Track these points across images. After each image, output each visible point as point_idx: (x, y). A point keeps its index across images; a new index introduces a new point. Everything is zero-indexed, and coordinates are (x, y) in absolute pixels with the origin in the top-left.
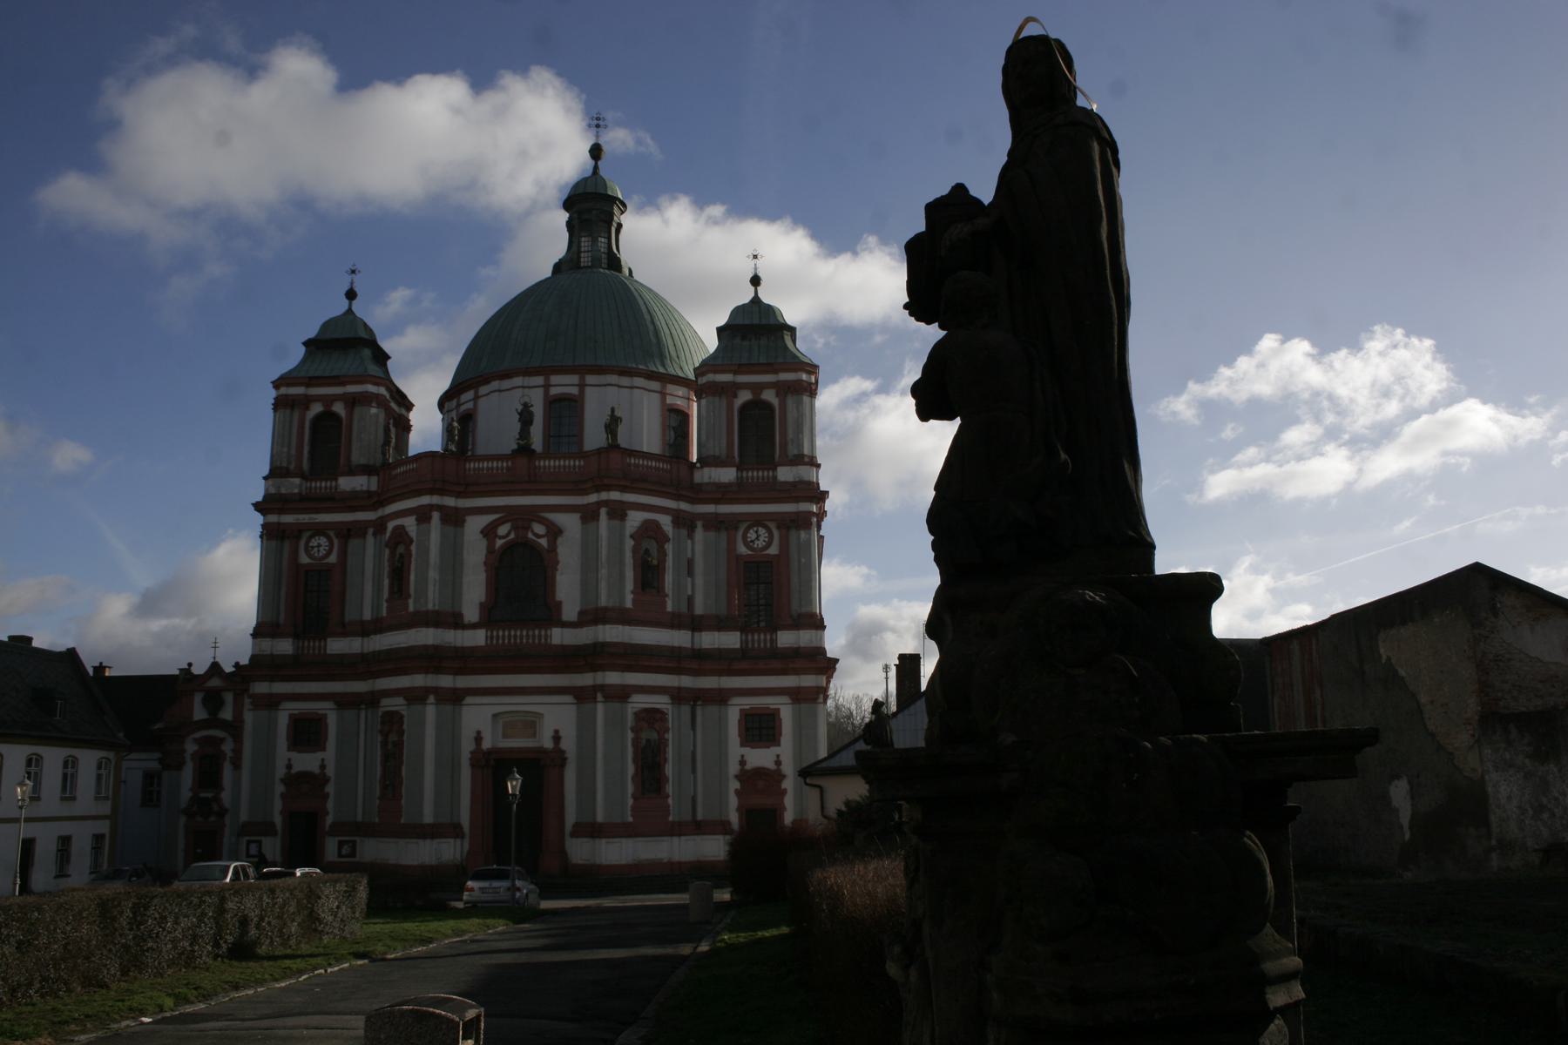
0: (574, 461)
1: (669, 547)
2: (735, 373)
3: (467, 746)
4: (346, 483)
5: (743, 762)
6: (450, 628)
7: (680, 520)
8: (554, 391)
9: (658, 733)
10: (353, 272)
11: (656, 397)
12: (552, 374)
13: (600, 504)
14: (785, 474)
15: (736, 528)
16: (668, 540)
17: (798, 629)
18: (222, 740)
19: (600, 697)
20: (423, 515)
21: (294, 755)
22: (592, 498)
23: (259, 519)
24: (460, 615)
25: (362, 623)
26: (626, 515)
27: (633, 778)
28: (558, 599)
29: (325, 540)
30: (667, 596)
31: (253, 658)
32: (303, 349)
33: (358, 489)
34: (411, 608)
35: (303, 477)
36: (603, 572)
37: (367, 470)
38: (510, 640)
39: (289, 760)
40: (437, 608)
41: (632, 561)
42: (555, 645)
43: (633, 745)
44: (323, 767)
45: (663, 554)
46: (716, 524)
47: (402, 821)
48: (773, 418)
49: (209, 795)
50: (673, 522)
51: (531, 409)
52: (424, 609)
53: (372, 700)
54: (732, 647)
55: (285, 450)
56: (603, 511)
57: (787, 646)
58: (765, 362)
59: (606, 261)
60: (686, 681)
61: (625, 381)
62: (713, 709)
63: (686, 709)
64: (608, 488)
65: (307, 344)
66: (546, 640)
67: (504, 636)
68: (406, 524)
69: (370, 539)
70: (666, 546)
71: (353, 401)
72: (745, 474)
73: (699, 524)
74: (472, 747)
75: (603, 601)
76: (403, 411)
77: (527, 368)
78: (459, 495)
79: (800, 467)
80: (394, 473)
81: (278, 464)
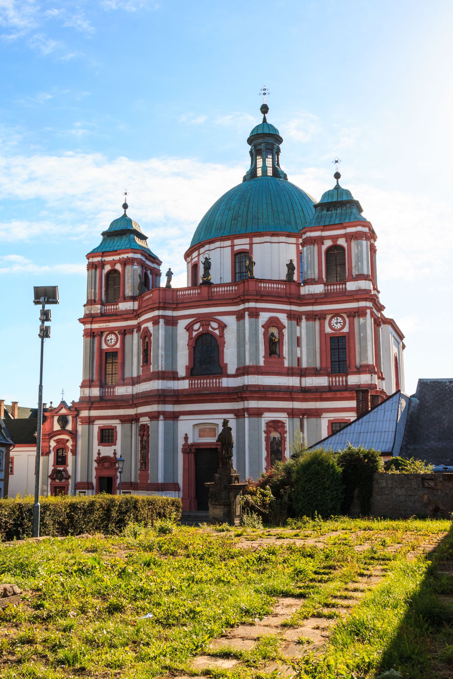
0: (232, 287)
1: (285, 332)
2: (322, 230)
3: (181, 442)
4: (123, 306)
6: (170, 380)
7: (291, 316)
8: (236, 248)
9: (280, 434)
10: (126, 194)
11: (295, 246)
12: (234, 239)
13: (245, 310)
14: (351, 286)
15: (325, 319)
16: (285, 327)
17: (360, 374)
18: (68, 441)
19: (246, 415)
20: (155, 321)
21: (101, 448)
22: (241, 307)
23: (82, 327)
24: (177, 373)
25: (132, 378)
26: (259, 315)
27: (266, 459)
28: (225, 362)
29: (114, 336)
30: (284, 358)
31: (82, 399)
32: (101, 237)
33: (128, 309)
34: (151, 371)
35: (102, 304)
36: (247, 347)
37: (133, 299)
38: (201, 385)
39: (99, 450)
40: (163, 369)
41: (263, 340)
42: (224, 387)
43: (266, 440)
44: (115, 454)
45: (281, 335)
46: (311, 316)
47: (149, 482)
48: (345, 255)
49: (61, 469)
50: (287, 317)
51: (209, 260)
52: (157, 370)
53: (135, 419)
54: (322, 385)
55: (93, 290)
56: (247, 313)
57: (354, 384)
58: (338, 223)
59: (271, 172)
60: (297, 405)
61: (275, 239)
62: (313, 420)
63: (297, 421)
64: (248, 301)
65: (103, 234)
66: (219, 384)
67: (198, 383)
68: (148, 326)
69: (136, 335)
70: (283, 331)
71: (125, 263)
72: (329, 288)
73: (304, 317)
74: (183, 442)
75: (247, 363)
76: (155, 266)
77: (222, 237)
78: (174, 309)
79: (359, 281)
80: (143, 299)
81: (90, 298)
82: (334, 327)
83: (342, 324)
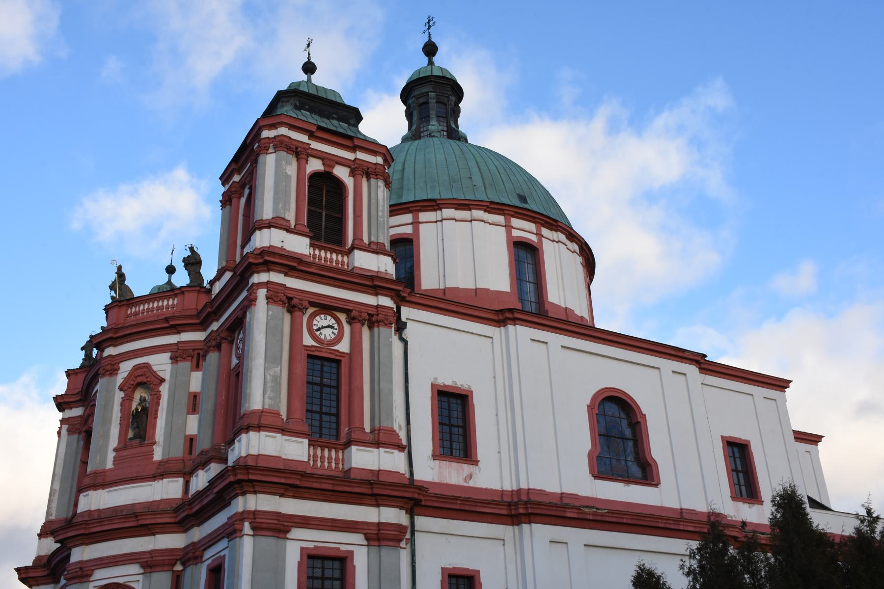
15: (303, 310)
82: (318, 333)
83: (336, 332)
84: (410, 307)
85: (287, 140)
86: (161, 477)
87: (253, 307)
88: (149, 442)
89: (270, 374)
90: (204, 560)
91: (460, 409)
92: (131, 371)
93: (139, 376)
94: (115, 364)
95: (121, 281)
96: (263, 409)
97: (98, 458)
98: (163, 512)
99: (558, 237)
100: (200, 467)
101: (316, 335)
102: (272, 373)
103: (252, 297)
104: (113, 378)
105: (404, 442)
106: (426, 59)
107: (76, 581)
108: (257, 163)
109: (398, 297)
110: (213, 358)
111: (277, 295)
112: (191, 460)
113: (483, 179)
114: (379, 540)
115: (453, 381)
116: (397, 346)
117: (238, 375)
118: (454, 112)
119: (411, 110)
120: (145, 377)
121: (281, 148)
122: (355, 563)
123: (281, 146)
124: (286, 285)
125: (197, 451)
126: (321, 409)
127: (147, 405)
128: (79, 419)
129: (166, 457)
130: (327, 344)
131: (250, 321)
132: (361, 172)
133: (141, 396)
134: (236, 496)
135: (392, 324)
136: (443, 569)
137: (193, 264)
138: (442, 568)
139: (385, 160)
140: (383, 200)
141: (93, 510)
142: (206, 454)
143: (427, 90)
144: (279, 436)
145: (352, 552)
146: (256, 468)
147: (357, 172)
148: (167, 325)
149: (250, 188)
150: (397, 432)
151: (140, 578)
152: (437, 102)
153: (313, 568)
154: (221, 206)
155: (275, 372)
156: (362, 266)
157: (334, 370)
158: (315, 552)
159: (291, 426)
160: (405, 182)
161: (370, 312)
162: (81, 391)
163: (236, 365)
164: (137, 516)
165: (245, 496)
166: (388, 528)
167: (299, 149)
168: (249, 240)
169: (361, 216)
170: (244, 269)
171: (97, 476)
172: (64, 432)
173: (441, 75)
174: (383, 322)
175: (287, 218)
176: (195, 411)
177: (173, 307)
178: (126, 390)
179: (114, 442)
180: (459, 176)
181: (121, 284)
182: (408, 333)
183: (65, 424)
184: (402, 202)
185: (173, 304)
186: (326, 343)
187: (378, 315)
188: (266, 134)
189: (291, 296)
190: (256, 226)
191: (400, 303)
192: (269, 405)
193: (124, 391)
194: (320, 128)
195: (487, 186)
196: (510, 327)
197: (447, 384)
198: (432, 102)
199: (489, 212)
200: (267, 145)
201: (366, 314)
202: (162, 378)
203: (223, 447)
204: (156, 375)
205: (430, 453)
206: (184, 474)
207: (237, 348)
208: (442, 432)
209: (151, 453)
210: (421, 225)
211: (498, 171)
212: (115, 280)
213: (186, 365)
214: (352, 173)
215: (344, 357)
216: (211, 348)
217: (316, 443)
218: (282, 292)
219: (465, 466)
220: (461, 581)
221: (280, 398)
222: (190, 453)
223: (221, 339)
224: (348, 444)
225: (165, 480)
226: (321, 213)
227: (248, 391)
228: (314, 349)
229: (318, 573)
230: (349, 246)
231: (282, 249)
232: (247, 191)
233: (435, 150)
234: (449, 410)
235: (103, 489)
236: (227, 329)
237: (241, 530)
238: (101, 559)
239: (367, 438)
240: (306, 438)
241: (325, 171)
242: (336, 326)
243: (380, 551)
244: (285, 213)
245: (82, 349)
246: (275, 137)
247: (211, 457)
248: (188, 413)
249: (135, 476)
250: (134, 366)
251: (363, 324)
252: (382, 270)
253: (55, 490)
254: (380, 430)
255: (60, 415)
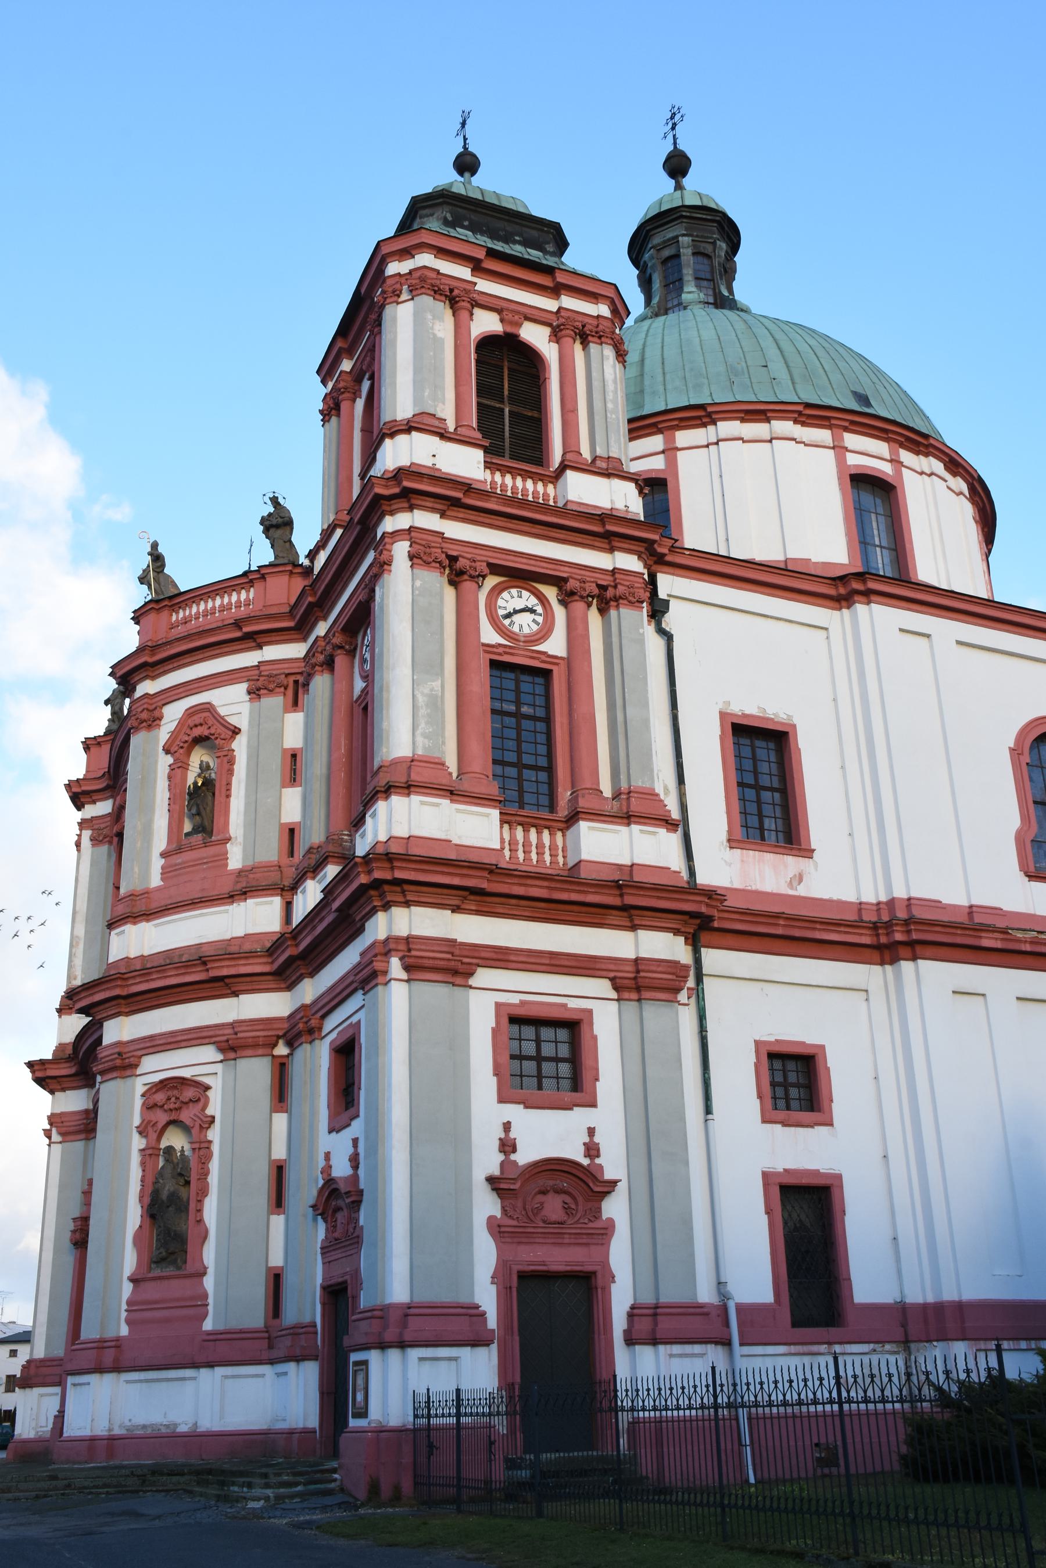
5: (507, 1146)
82: (507, 622)
83: (540, 619)
84: (673, 574)
85: (433, 275)
86: (243, 897)
87: (386, 576)
88: (219, 838)
89: (422, 694)
90: (323, 1034)
91: (773, 758)
92: (181, 718)
93: (196, 726)
94: (156, 708)
95: (158, 567)
96: (414, 756)
97: (136, 870)
98: (251, 955)
99: (931, 466)
100: (309, 874)
101: (504, 625)
102: (426, 691)
103: (383, 557)
104: (154, 732)
105: (675, 815)
106: (672, 183)
107: (115, 1074)
108: (380, 325)
109: (651, 555)
110: (321, 683)
111: (428, 550)
112: (292, 866)
113: (788, 367)
114: (638, 989)
115: (759, 708)
116: (655, 644)
117: (365, 709)
118: (726, 271)
119: (649, 271)
120: (207, 727)
121: (423, 290)
122: (597, 1030)
123: (423, 287)
124: (443, 534)
125: (300, 850)
126: (519, 757)
127: (213, 776)
128: (109, 819)
129: (250, 863)
130: (524, 642)
131: (382, 599)
132: (572, 333)
133: (202, 762)
134: (373, 912)
135: (642, 602)
136: (757, 1043)
137: (277, 526)
138: (755, 1041)
139: (615, 311)
140: (615, 381)
141: (132, 957)
142: (318, 852)
143: (675, 234)
144: (445, 802)
145: (590, 1012)
146: (406, 858)
147: (563, 332)
148: (238, 634)
149: (372, 378)
150: (662, 797)
151: (219, 1068)
152: (694, 254)
153: (520, 1040)
154: (322, 420)
155: (432, 690)
156: (581, 498)
157: (540, 690)
158: (522, 1012)
159: (466, 786)
160: (647, 382)
161: (600, 582)
162: (109, 771)
163: (362, 691)
164: (205, 963)
165: (389, 912)
166: (654, 968)
167: (456, 292)
168: (374, 459)
169: (575, 410)
170: (365, 510)
171: (136, 901)
172: (86, 842)
173: (700, 204)
174: (626, 599)
175: (440, 415)
176: (294, 781)
177: (247, 605)
178: (175, 752)
179: (160, 841)
180: (744, 364)
181: (158, 573)
182: (671, 620)
183: (87, 828)
184: (644, 413)
185: (247, 599)
186: (522, 639)
187: (615, 587)
188: (394, 268)
189: (455, 554)
190: (384, 431)
191: (654, 568)
192: (424, 748)
193: (172, 754)
194: (492, 253)
195: (797, 379)
196: (860, 608)
197: (747, 712)
198: (686, 253)
199: (804, 424)
200: (398, 286)
201: (594, 585)
202: (235, 727)
203: (346, 837)
204: (227, 725)
205: (724, 836)
206: (282, 890)
207: (363, 661)
208: (743, 799)
209: (224, 857)
210: (679, 454)
211: (815, 354)
212: (148, 566)
213: (274, 702)
214: (556, 336)
215: (557, 664)
216: (317, 668)
217: (513, 819)
218: (438, 545)
219: (790, 860)
220: (791, 1065)
221: (443, 736)
222: (291, 854)
223: (333, 649)
224: (573, 819)
225: (250, 902)
226: (502, 410)
227: (385, 725)
228: (501, 650)
229: (530, 1048)
230: (557, 466)
231: (433, 468)
232: (366, 385)
233: (697, 324)
234: (754, 758)
235: (148, 921)
236: (342, 630)
237: (385, 973)
238: (151, 1038)
239: (608, 807)
240: (495, 807)
241: (505, 332)
242: (539, 609)
243: (641, 1009)
244: (436, 406)
245: (107, 702)
246: (411, 272)
247: (327, 854)
248: (284, 786)
249: (200, 896)
250: (186, 710)
251: (589, 605)
252: (620, 505)
253: (77, 937)
254: (629, 792)
255: (78, 816)
